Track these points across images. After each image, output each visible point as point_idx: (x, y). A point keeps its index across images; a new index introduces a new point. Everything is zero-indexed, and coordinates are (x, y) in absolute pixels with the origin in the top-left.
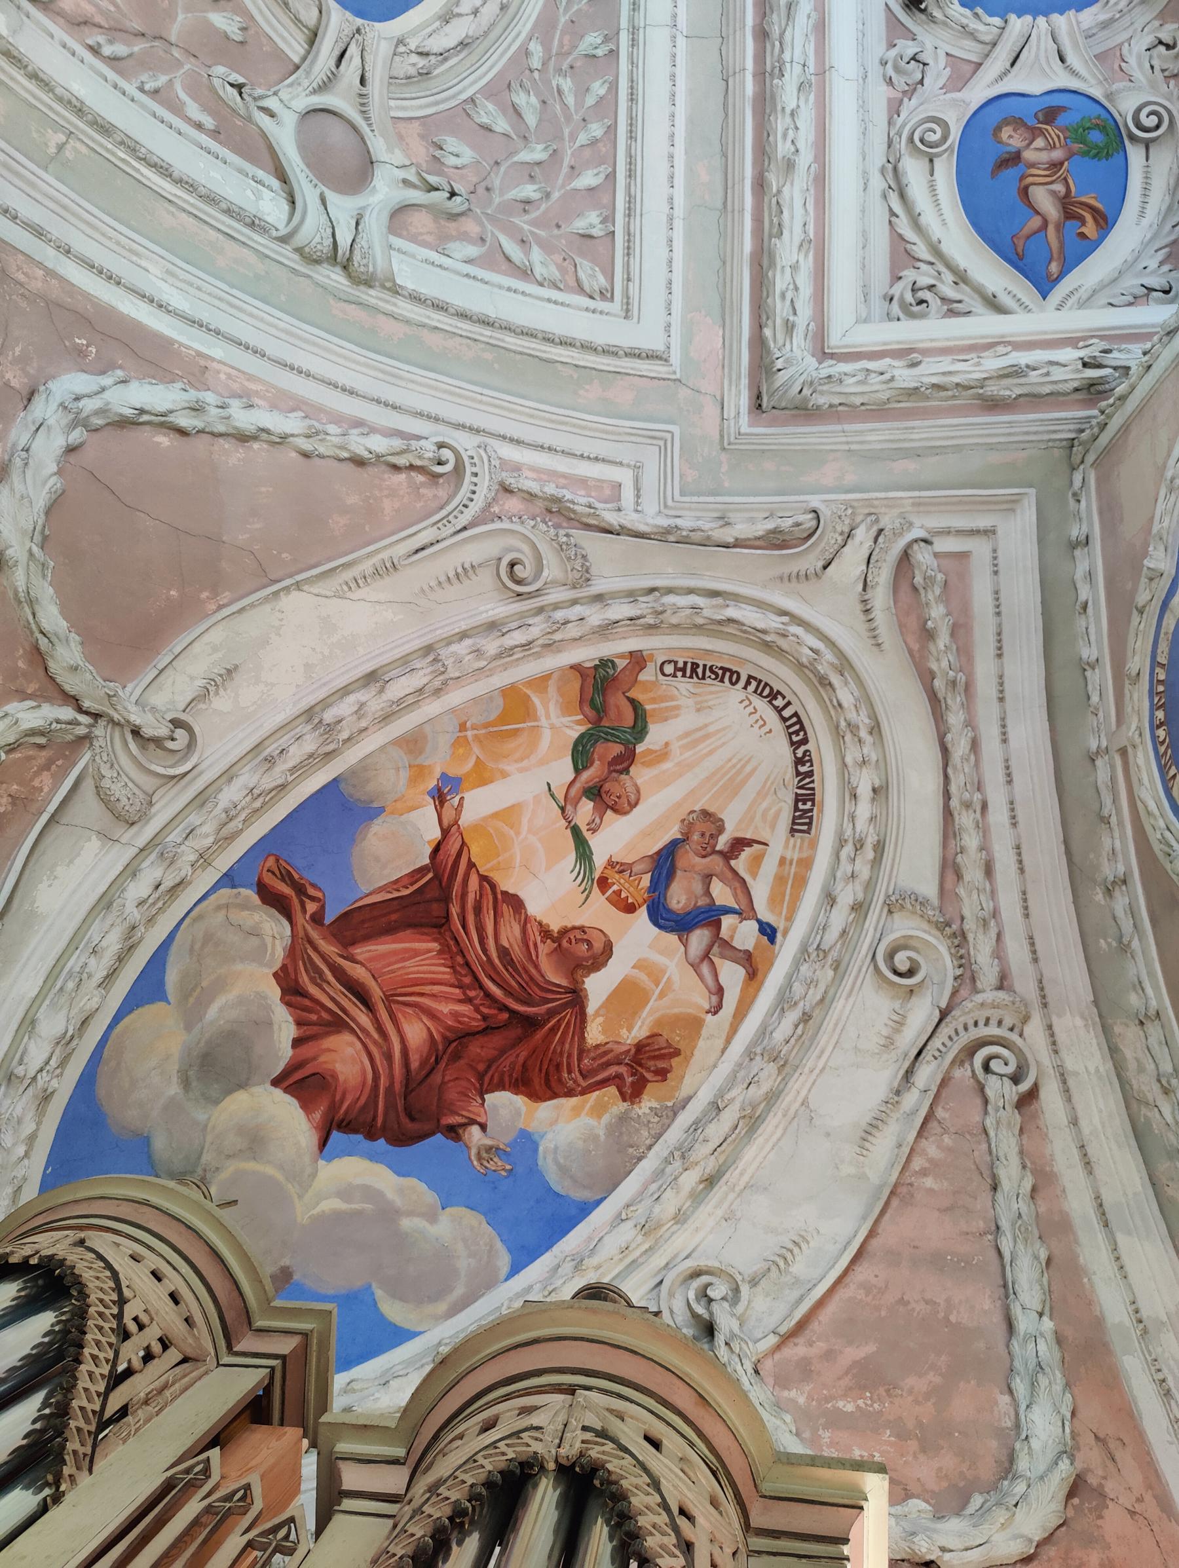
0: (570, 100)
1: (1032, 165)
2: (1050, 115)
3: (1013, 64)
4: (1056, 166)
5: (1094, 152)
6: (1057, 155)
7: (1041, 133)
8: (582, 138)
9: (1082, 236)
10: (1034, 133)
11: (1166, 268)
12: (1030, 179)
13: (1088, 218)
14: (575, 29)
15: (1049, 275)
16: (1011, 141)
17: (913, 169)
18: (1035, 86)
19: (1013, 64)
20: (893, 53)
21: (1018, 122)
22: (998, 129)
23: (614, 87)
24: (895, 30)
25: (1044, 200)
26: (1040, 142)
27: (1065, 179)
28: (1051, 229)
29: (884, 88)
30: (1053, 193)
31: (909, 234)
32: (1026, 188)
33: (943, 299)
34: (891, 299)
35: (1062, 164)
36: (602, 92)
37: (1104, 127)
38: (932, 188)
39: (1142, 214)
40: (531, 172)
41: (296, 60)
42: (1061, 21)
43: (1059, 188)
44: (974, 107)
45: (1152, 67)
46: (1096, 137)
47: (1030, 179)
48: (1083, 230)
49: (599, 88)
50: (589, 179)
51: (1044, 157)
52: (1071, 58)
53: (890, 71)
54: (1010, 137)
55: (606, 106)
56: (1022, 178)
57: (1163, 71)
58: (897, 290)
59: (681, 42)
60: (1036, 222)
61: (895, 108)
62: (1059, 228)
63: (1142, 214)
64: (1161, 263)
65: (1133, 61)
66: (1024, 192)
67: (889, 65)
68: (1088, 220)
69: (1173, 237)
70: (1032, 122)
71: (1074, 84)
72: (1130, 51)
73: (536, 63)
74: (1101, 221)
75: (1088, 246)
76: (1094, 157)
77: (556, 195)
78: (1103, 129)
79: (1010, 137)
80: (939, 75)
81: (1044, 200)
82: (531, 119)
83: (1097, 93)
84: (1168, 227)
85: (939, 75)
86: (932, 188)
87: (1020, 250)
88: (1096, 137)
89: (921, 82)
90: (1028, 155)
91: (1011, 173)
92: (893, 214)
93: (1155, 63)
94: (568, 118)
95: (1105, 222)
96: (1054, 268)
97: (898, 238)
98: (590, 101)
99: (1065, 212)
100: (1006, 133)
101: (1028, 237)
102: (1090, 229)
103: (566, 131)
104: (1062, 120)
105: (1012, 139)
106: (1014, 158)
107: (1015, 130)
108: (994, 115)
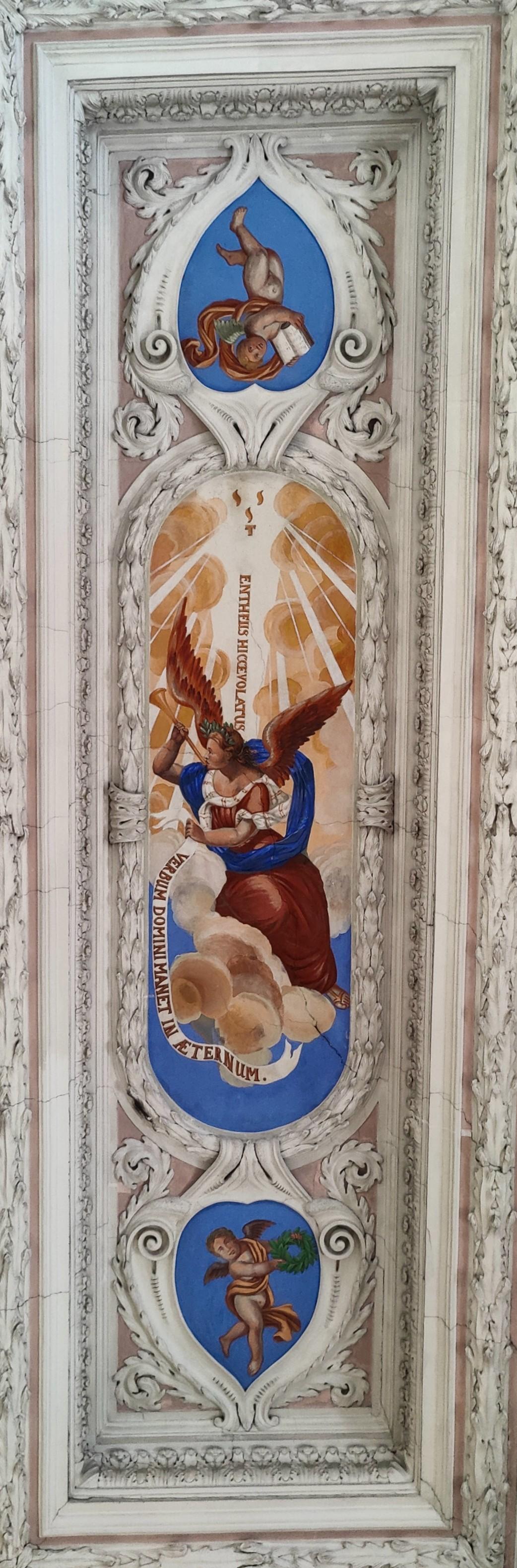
1: (239, 1277)
2: (256, 1228)
3: (226, 1178)
4: (257, 1278)
5: (291, 1266)
6: (260, 1269)
7: (248, 1247)
9: (279, 1339)
10: (242, 1247)
11: (346, 1367)
12: (236, 1289)
13: (284, 1324)
15: (249, 1372)
16: (221, 1253)
17: (137, 1268)
18: (246, 1196)
19: (226, 1178)
20: (123, 1152)
21: (227, 1234)
22: (211, 1240)
24: (126, 1133)
25: (247, 1308)
26: (246, 1256)
27: (266, 1291)
28: (252, 1335)
29: (115, 1185)
30: (255, 1303)
31: (132, 1324)
32: (233, 1297)
33: (160, 1385)
34: (118, 1383)
35: (263, 1277)
37: (302, 1242)
38: (154, 1285)
39: (330, 1317)
42: (267, 1150)
43: (260, 1298)
44: (192, 1214)
45: (346, 1184)
46: (294, 1251)
47: (236, 1289)
48: (280, 1334)
51: (249, 1270)
52: (276, 1177)
53: (121, 1172)
54: (221, 1248)
56: (230, 1287)
57: (355, 1187)
58: (122, 1376)
60: (239, 1328)
61: (123, 1209)
62: (258, 1333)
63: (330, 1317)
64: (343, 1363)
65: (330, 1177)
66: (231, 1300)
67: (120, 1165)
68: (284, 1325)
69: (354, 1341)
70: (239, 1235)
71: (279, 1197)
72: (329, 1169)
74: (295, 1325)
75: (283, 1348)
76: (291, 1271)
78: (300, 1243)
79: (221, 1248)
80: (162, 1179)
81: (247, 1308)
83: (296, 1205)
84: (350, 1333)
85: (162, 1179)
86: (154, 1285)
87: (226, 1349)
88: (294, 1251)
89: (147, 1182)
90: (237, 1268)
91: (220, 1283)
92: (120, 1306)
93: (349, 1180)
95: (299, 1326)
96: (254, 1366)
97: (123, 1326)
99: (264, 1320)
100: (218, 1243)
101: (234, 1339)
102: (285, 1333)
104: (268, 1234)
105: (223, 1251)
106: (221, 1270)
107: (225, 1242)
108: (208, 1228)
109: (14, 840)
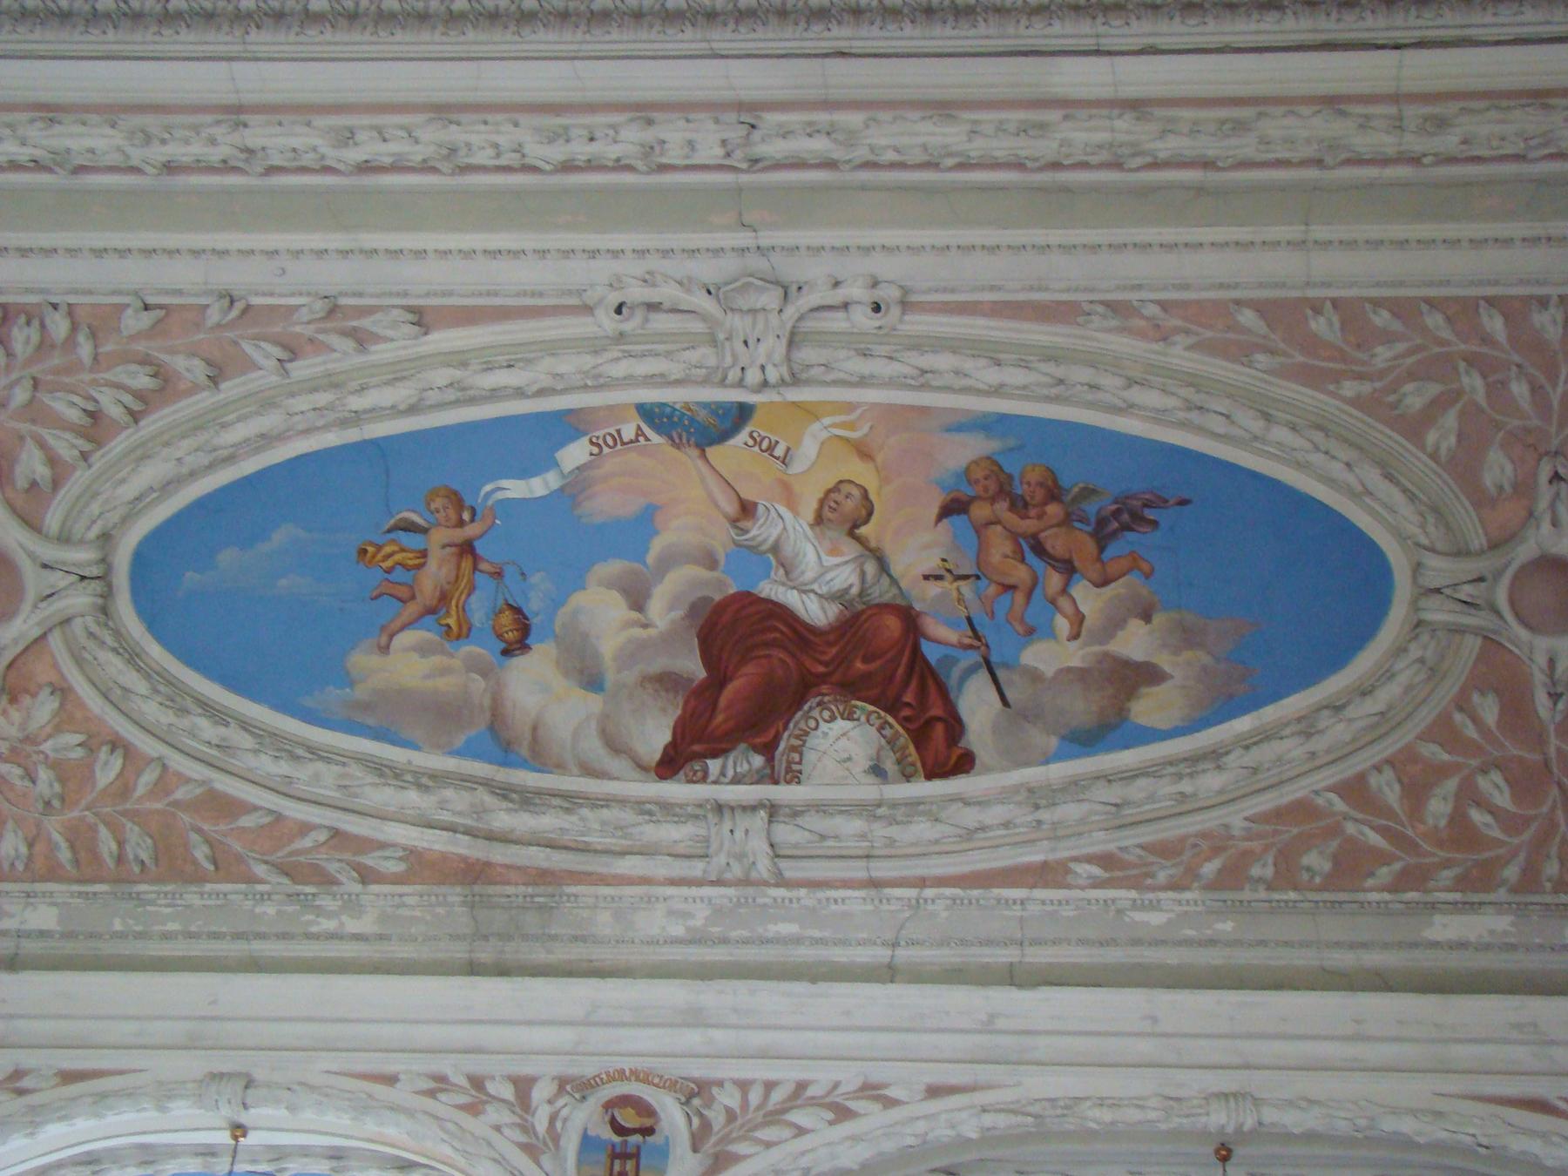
0: (1400, 347)
8: (1446, 334)
14: (1312, 344)
23: (1377, 303)
36: (1385, 314)
40: (1497, 390)
41: (1479, 641)
49: (1382, 319)
50: (1495, 325)
55: (1400, 308)
59: (1320, 232)
73: (1366, 388)
77: (1516, 358)
82: (1434, 389)
94: (1418, 349)
98: (1397, 326)
103: (1437, 350)
109: (756, 135)
